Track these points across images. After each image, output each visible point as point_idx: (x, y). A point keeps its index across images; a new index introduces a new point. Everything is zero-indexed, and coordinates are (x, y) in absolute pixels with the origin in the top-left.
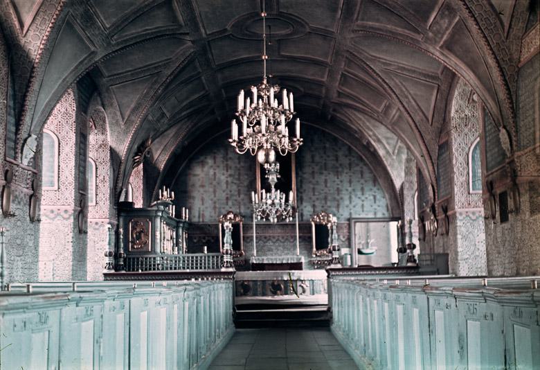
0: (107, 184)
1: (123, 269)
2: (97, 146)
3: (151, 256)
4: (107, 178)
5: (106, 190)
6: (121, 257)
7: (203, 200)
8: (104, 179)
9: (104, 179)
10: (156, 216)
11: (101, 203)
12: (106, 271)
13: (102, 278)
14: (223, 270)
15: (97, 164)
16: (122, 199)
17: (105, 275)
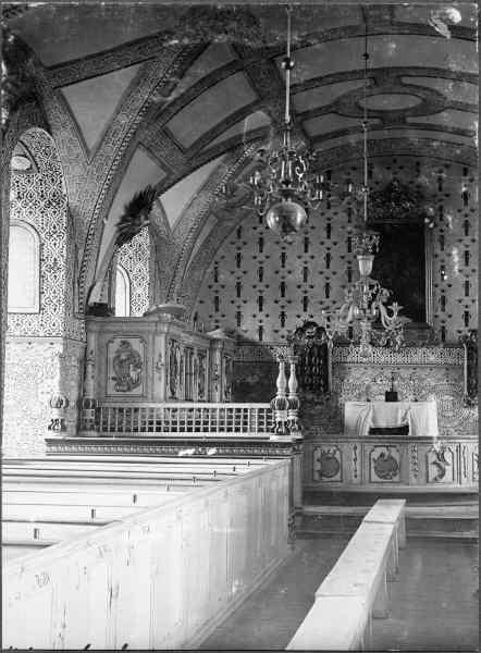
0: (61, 274)
1: (92, 428)
2: (42, 204)
3: (145, 405)
4: (61, 262)
5: (59, 283)
6: (87, 406)
7: (261, 301)
8: (55, 263)
9: (55, 263)
10: (156, 333)
11: (49, 309)
12: (52, 435)
13: (41, 450)
14: (274, 438)
15: (43, 236)
16: (95, 298)
17: (50, 442)
